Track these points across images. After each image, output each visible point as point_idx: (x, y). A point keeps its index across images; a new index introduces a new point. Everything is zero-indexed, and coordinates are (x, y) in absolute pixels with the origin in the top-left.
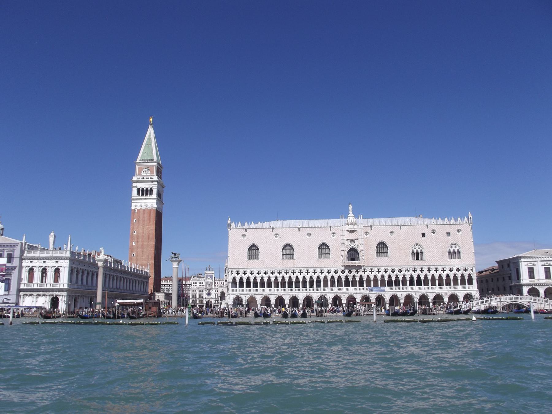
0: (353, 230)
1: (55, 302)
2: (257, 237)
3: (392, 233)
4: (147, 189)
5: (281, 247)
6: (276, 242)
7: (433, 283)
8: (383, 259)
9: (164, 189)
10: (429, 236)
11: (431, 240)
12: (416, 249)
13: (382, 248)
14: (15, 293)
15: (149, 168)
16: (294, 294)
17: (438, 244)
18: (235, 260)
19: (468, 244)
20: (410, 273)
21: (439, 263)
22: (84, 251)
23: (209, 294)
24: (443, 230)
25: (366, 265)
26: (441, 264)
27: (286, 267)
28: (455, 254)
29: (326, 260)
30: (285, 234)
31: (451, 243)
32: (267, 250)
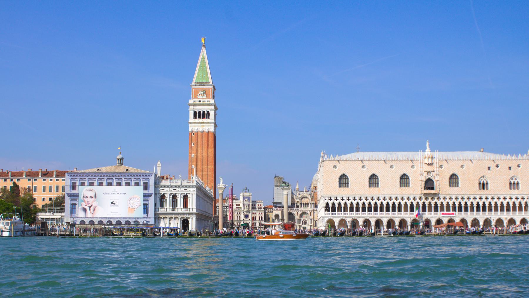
0: (430, 163)
1: (185, 224)
2: (347, 168)
3: (462, 166)
4: (204, 112)
6: (363, 172)
9: (216, 111)
13: (453, 179)
14: (153, 216)
15: (205, 91)
16: (380, 217)
18: (328, 187)
20: (477, 201)
23: (247, 216)
25: (441, 193)
26: (503, 193)
27: (373, 194)
32: (355, 179)
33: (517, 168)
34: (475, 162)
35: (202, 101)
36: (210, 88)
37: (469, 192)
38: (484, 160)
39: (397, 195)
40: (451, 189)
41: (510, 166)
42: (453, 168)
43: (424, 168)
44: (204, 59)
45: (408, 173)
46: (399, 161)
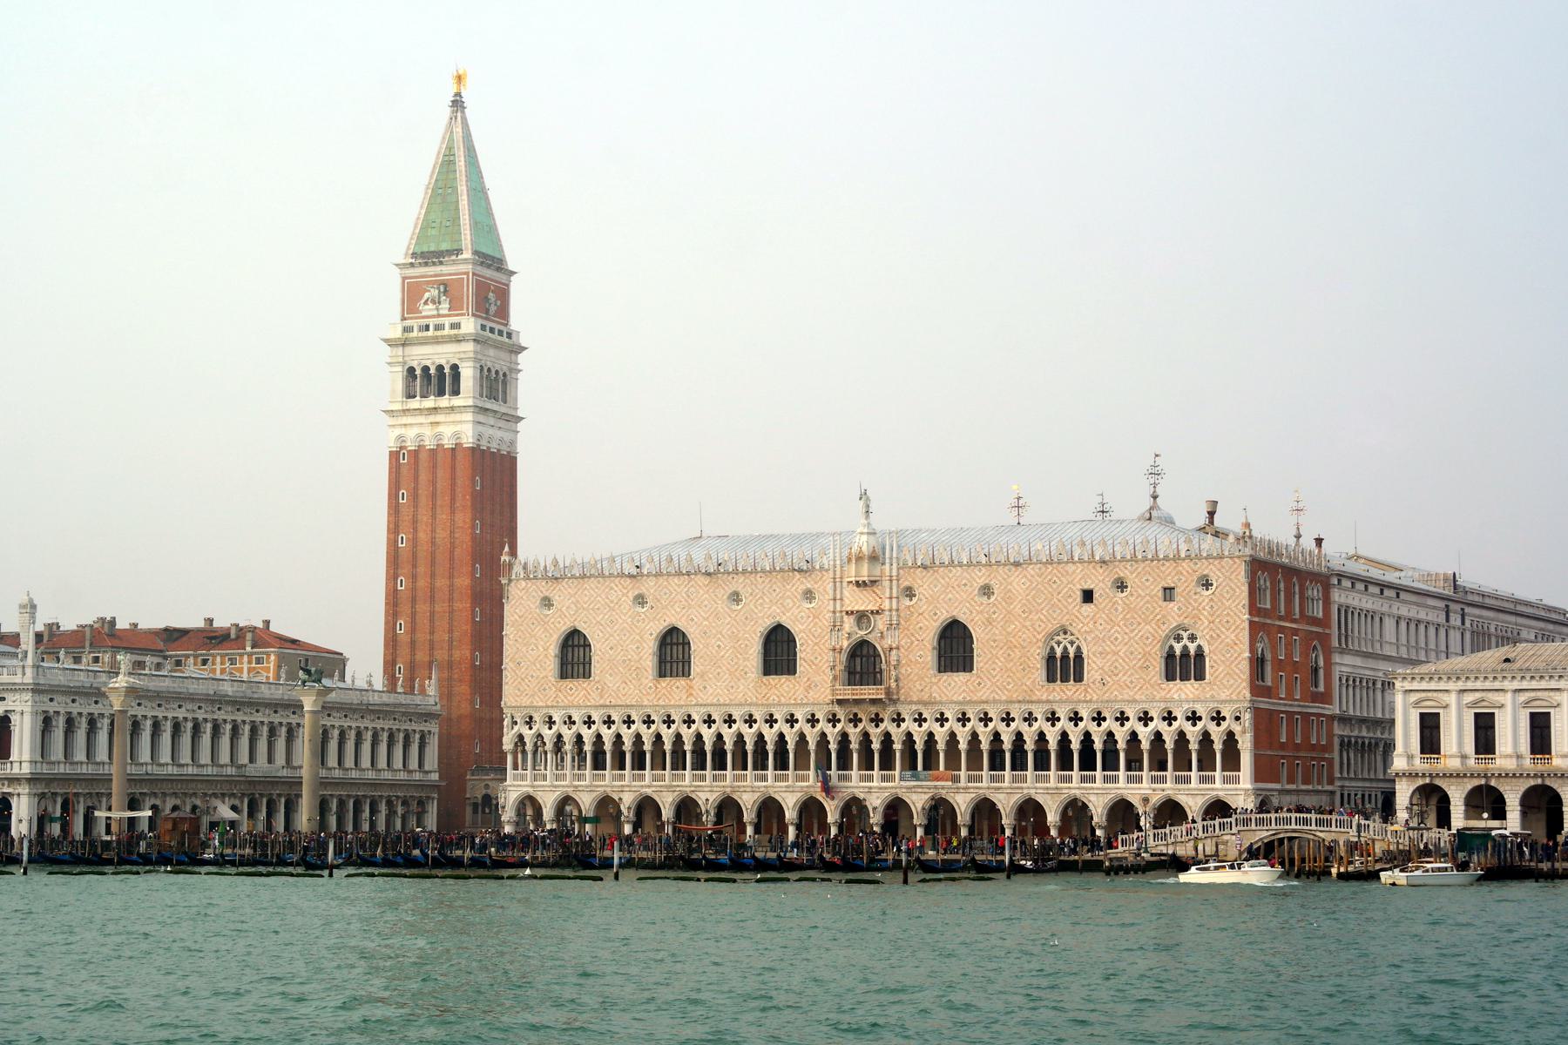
0: (864, 582)
3: (986, 591)
4: (440, 368)
6: (638, 621)
7: (1110, 763)
8: (956, 679)
9: (521, 358)
10: (1107, 601)
11: (1111, 613)
12: (1061, 646)
15: (445, 285)
16: (688, 789)
19: (1233, 627)
21: (1131, 694)
22: (212, 625)
24: (1152, 580)
25: (902, 698)
26: (1137, 697)
29: (783, 680)
31: (1175, 624)
32: (611, 648)
33: (1195, 594)
34: (1032, 572)
35: (431, 328)
36: (465, 273)
38: (1067, 562)
39: (750, 705)
40: (940, 680)
42: (950, 596)
43: (847, 601)
44: (452, 158)
45: (788, 621)
46: (759, 575)
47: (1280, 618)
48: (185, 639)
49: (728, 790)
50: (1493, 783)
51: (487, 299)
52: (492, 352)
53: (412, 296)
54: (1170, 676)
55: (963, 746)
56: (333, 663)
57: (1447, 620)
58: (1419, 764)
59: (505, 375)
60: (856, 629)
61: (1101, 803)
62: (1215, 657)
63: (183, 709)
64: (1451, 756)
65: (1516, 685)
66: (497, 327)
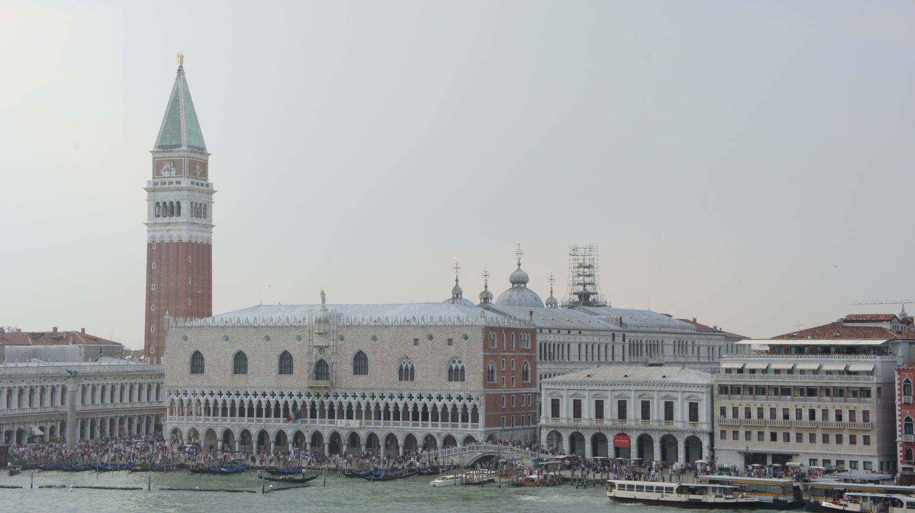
0: (321, 333)
2: (202, 340)
3: (374, 338)
4: (171, 203)
5: (232, 355)
9: (214, 196)
16: (245, 426)
17: (434, 357)
22: (57, 331)
24: (443, 335)
25: (338, 386)
26: (436, 388)
28: (456, 374)
29: (287, 377)
30: (237, 336)
31: (452, 356)
32: (213, 360)
33: (461, 342)
35: (167, 183)
37: (382, 384)
39: (273, 387)
41: (450, 337)
43: (315, 341)
44: (178, 98)
47: (503, 352)
48: (42, 338)
49: (263, 427)
50: (580, 431)
51: (195, 168)
52: (197, 195)
53: (158, 167)
54: (450, 379)
55: (363, 409)
56: (115, 350)
57: (613, 340)
58: (551, 422)
59: (205, 205)
60: (318, 354)
61: (421, 436)
62: (468, 371)
63: (24, 382)
64: (564, 419)
65: (590, 388)
66: (200, 182)
